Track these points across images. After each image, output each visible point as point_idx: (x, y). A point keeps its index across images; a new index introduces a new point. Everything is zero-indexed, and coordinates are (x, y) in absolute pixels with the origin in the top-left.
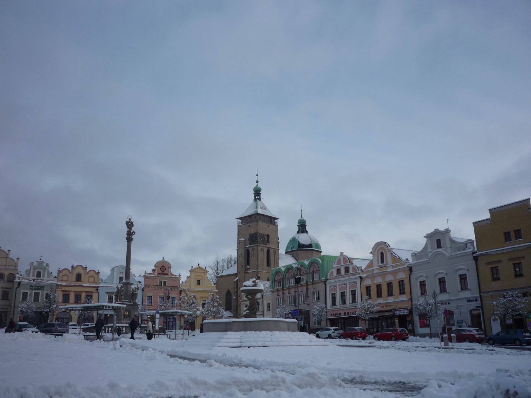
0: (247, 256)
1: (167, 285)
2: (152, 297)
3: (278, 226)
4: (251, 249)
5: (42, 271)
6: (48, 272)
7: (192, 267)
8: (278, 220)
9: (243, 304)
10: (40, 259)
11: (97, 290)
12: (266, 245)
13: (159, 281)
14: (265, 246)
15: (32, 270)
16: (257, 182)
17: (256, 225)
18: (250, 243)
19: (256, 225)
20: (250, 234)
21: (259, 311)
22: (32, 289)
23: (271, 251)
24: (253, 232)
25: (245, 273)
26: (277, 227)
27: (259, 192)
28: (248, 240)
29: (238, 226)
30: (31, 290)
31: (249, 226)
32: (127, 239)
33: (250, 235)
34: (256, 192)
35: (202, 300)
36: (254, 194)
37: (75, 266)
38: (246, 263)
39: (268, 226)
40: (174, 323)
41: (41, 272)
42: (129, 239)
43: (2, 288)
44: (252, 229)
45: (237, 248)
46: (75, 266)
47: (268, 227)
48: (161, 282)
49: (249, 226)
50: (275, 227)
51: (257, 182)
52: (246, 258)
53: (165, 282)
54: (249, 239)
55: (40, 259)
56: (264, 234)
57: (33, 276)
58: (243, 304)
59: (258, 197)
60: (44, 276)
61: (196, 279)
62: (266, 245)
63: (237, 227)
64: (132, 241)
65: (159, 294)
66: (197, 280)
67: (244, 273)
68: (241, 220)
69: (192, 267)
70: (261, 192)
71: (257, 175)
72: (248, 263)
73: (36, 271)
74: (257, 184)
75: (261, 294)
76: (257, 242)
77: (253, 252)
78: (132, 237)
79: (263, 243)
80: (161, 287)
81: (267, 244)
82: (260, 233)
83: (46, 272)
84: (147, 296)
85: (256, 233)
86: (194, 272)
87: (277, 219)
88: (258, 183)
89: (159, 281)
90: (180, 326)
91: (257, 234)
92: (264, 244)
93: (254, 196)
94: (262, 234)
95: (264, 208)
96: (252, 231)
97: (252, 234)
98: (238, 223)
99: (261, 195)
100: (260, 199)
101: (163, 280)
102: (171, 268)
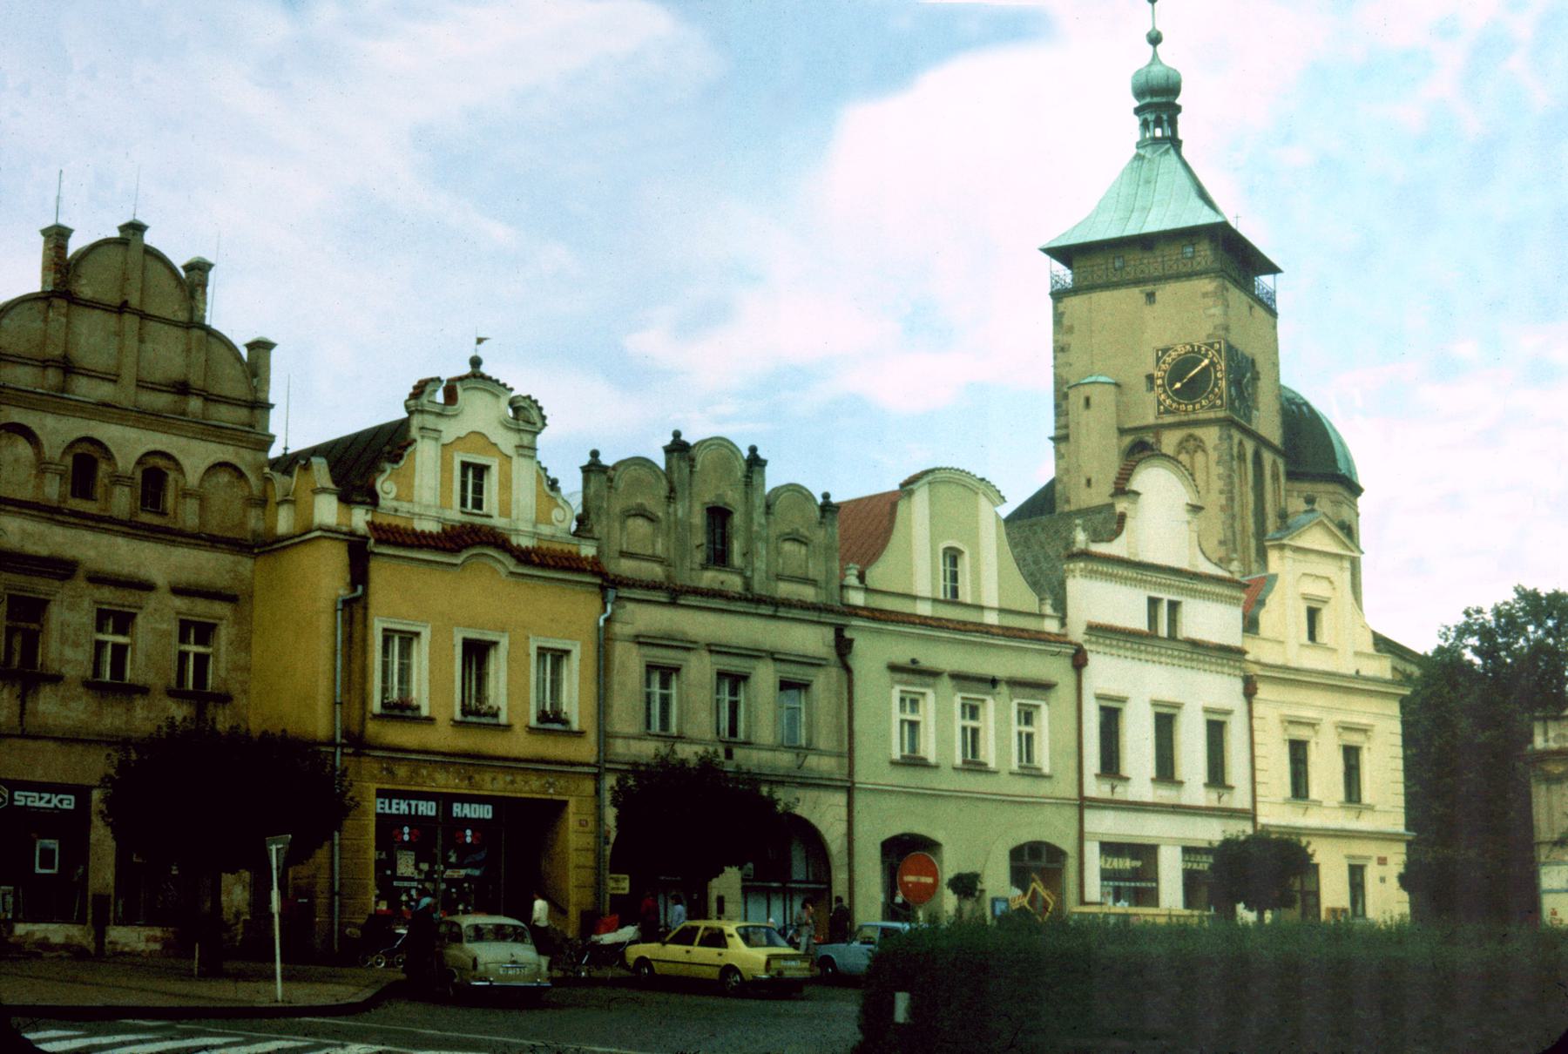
5: (495, 464)
11: (843, 646)
16: (1155, 40)
19: (1205, 295)
23: (1268, 457)
26: (1275, 327)
29: (1058, 295)
36: (1138, 111)
43: (177, 591)
48: (1153, 603)
49: (1151, 297)
51: (1155, 40)
53: (1174, 606)
54: (1150, 378)
55: (476, 362)
61: (1306, 597)
63: (1049, 302)
70: (1178, 101)
74: (1155, 51)
86: (1298, 549)
87: (1273, 269)
88: (1159, 47)
98: (1055, 280)
99: (1180, 117)
101: (1166, 596)
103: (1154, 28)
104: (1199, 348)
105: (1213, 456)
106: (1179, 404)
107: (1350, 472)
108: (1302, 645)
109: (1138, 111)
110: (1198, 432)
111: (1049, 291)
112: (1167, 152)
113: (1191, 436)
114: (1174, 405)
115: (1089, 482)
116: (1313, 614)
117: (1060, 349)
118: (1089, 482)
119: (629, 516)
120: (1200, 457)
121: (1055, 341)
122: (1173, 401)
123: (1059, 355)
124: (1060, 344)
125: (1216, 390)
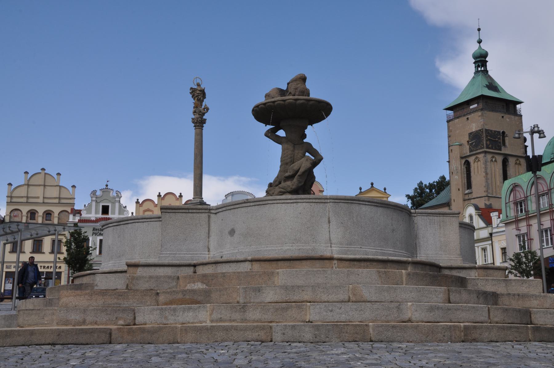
0: (467, 171)
3: (521, 116)
4: (474, 158)
5: (110, 205)
6: (120, 205)
7: (361, 189)
8: (522, 104)
10: (107, 186)
12: (500, 150)
14: (499, 152)
15: (94, 204)
16: (480, 42)
17: (479, 116)
18: (470, 148)
19: (479, 116)
20: (469, 134)
22: (96, 234)
24: (474, 130)
25: (464, 200)
26: (521, 119)
27: (483, 59)
28: (466, 143)
29: (448, 122)
30: (94, 235)
31: (468, 119)
32: (194, 121)
33: (469, 136)
34: (478, 60)
36: (474, 63)
37: (162, 195)
38: (466, 184)
39: (503, 117)
41: (108, 206)
42: (199, 123)
44: (474, 125)
45: (448, 160)
46: (162, 195)
47: (502, 119)
49: (468, 119)
50: (517, 118)
51: (480, 42)
52: (465, 175)
55: (107, 186)
56: (495, 131)
57: (96, 212)
59: (483, 68)
60: (113, 213)
62: (500, 150)
63: (446, 123)
64: (204, 125)
67: (462, 200)
68: (453, 112)
69: (361, 189)
70: (487, 59)
71: (479, 30)
72: (469, 186)
73: (101, 204)
74: (480, 46)
75: (488, 231)
76: (483, 145)
77: (476, 163)
78: (204, 117)
79: (494, 148)
81: (503, 148)
82: (486, 130)
83: (117, 205)
85: (480, 130)
87: (520, 103)
88: (481, 44)
91: (482, 132)
92: (496, 149)
93: (475, 67)
94: (491, 131)
95: (493, 86)
96: (474, 127)
97: (472, 133)
98: (448, 116)
99: (488, 64)
100: (486, 72)
102: (324, 192)
103: (480, 39)
104: (478, 131)
105: (482, 161)
106: (474, 148)
109: (474, 63)
110: (478, 156)
111: (446, 121)
112: (479, 75)
113: (477, 157)
114: (473, 149)
115: (452, 173)
117: (449, 136)
118: (452, 173)
119: (145, 211)
120: (479, 163)
121: (448, 134)
122: (473, 148)
123: (449, 138)
124: (449, 135)
125: (482, 143)
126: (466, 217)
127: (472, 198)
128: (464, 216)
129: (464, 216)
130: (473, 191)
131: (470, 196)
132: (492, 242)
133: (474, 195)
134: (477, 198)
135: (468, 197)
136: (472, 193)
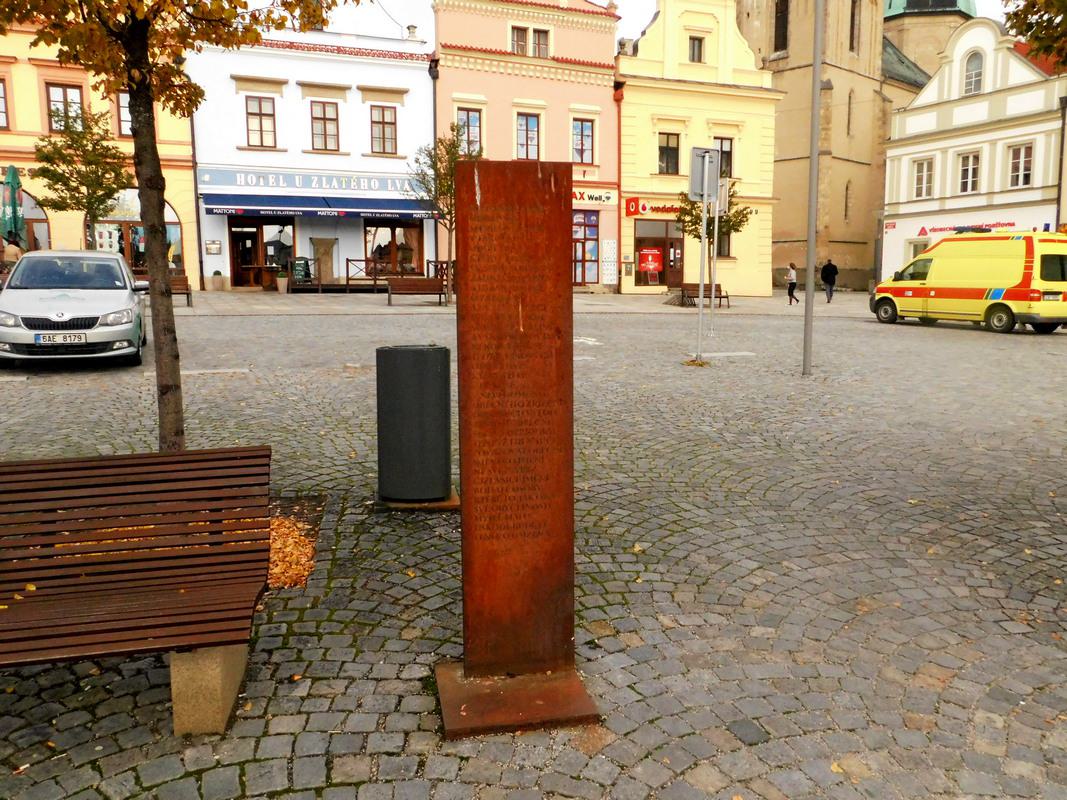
1: (552, 52)
2: (479, 111)
9: (899, 158)
13: (514, 28)
21: (924, 197)
35: (715, 138)
40: (589, 245)
48: (520, 31)
52: (774, 21)
58: (899, 158)
65: (516, 100)
66: (693, 39)
80: (524, 60)
84: (456, 105)
89: (514, 28)
90: (620, 263)
107: (969, 9)
108: (680, 64)
116: (697, 43)
126: (952, 61)
127: (788, 67)
128: (946, 57)
129: (946, 57)
130: (790, 53)
131: (782, 65)
132: (1064, 124)
133: (793, 62)
134: (799, 68)
135: (778, 65)
136: (787, 58)
